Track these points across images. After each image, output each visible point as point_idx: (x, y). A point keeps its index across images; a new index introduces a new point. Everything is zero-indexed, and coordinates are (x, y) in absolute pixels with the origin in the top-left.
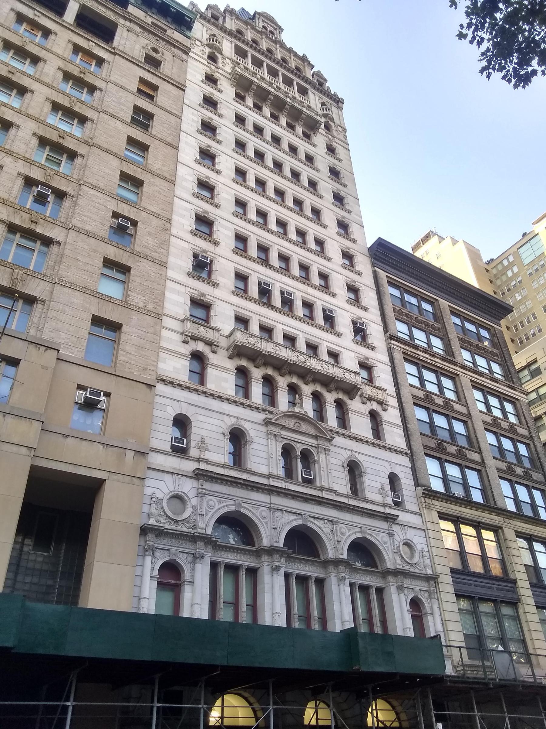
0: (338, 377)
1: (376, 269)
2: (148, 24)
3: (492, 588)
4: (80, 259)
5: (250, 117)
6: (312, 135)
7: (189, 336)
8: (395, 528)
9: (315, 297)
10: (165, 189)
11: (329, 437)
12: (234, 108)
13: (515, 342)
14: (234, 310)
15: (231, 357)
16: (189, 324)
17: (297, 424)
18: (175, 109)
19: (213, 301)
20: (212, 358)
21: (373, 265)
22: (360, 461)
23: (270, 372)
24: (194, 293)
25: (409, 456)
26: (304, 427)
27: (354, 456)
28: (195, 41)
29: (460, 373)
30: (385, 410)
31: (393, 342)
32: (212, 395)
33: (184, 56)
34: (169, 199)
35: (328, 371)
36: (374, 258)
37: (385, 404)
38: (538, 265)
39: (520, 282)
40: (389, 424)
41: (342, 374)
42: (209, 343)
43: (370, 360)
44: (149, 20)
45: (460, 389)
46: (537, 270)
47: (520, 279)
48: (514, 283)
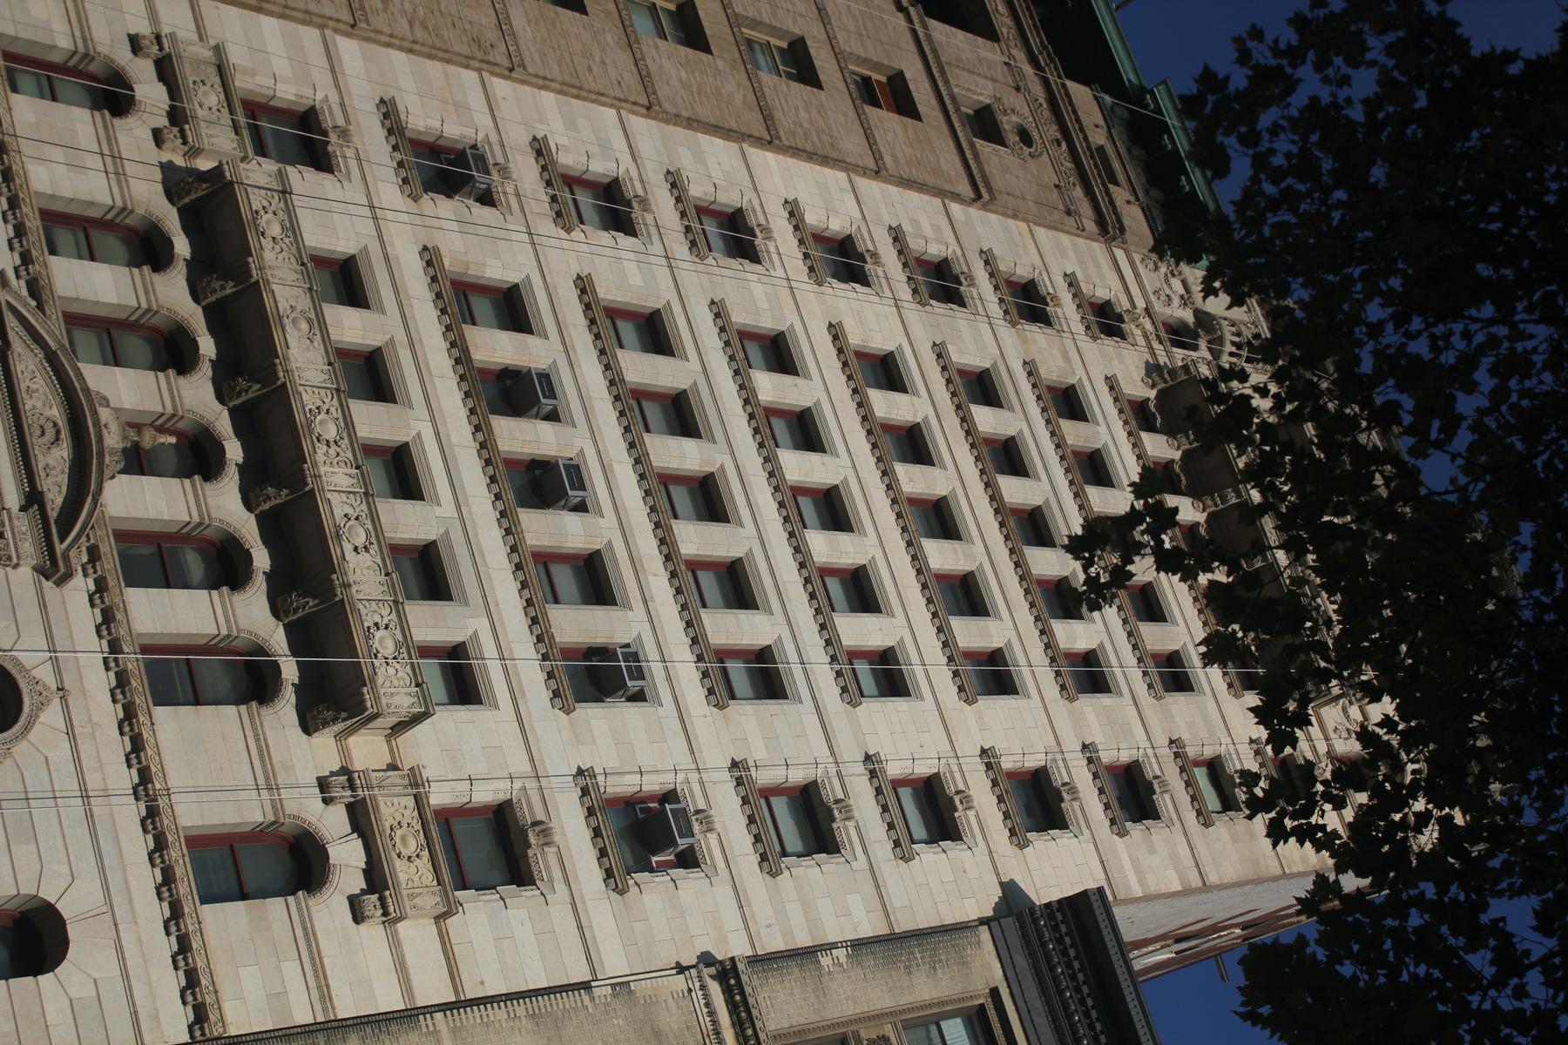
0: (347, 586)
2: (1089, 147)
5: (1102, 429)
7: (161, 49)
9: (645, 602)
10: (613, 74)
11: (60, 548)
12: (1080, 373)
14: (366, 248)
15: (175, 182)
16: (207, 54)
17: (50, 433)
18: (895, 158)
19: (349, 173)
20: (134, 133)
22: (27, 728)
23: (290, 670)
24: (331, 113)
25: (198, 1033)
26: (55, 461)
27: (41, 706)
28: (1173, 275)
30: (358, 914)
31: (715, 988)
32: (137, 745)
33: (1091, 226)
34: (591, 79)
35: (348, 547)
37: (382, 900)
40: (300, 933)
41: (377, 619)
42: (177, 117)
43: (551, 850)
44: (1099, 138)
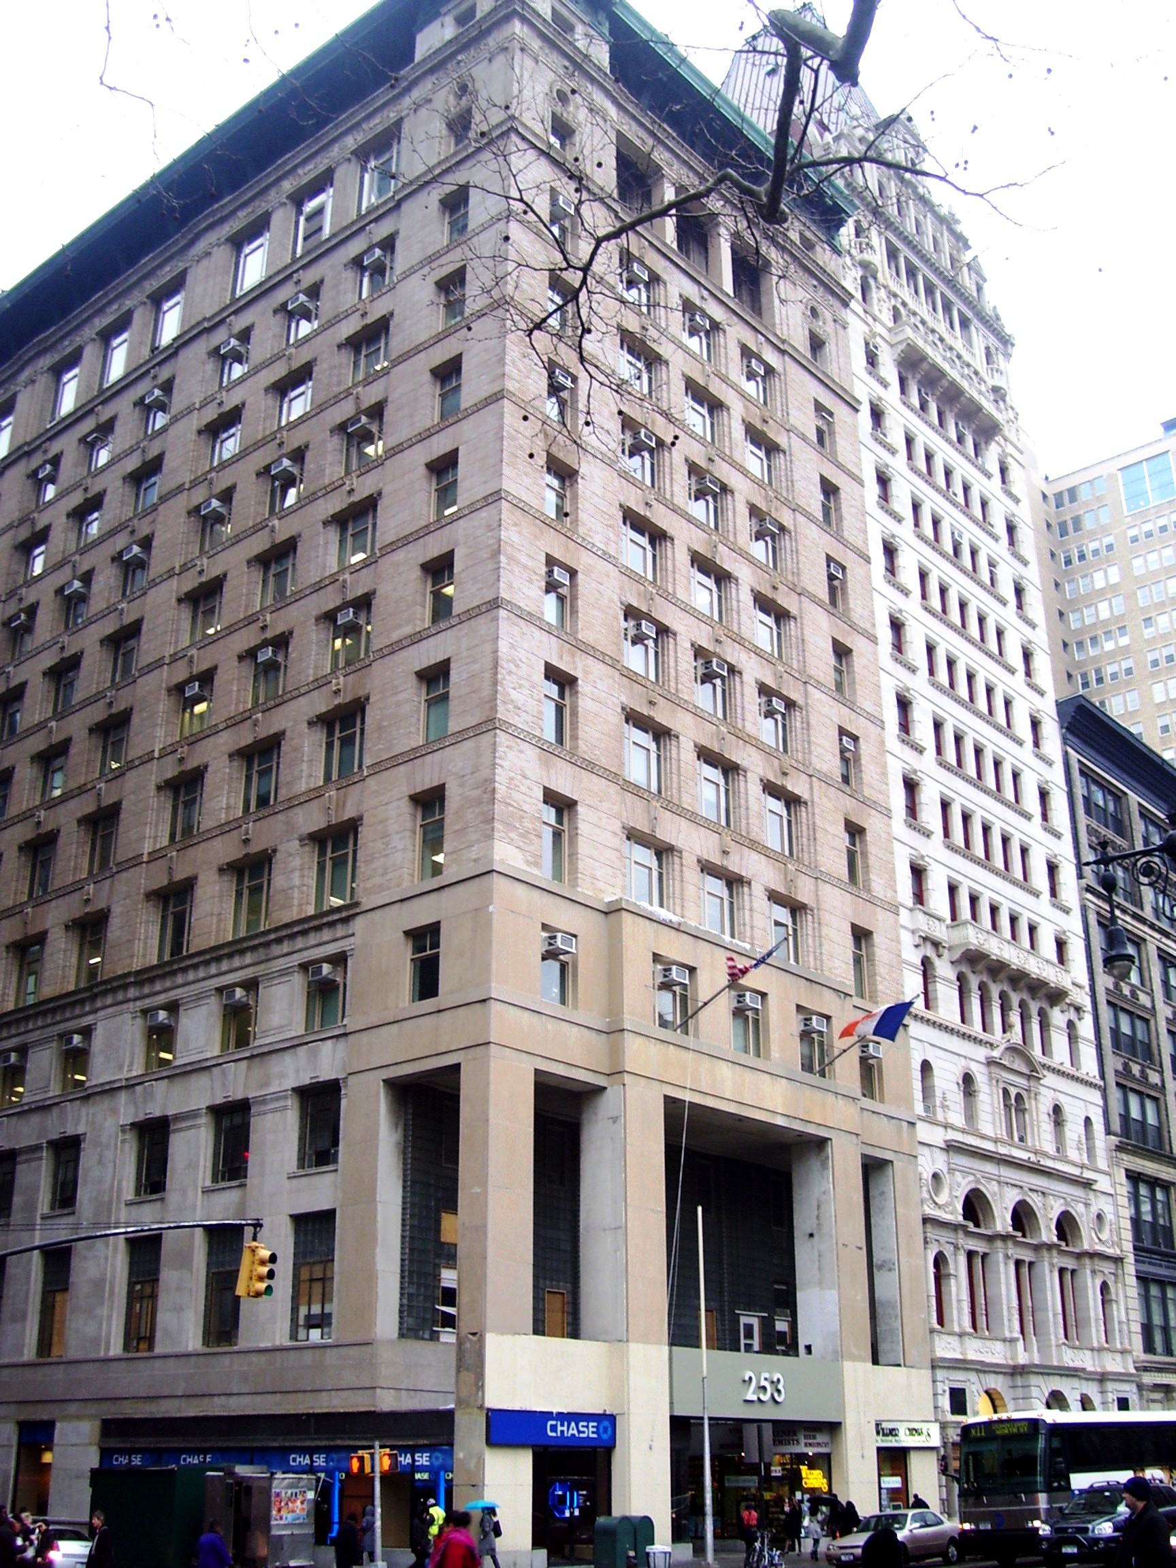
1: (1070, 750)
3: (1160, 1266)
4: (827, 827)
6: (983, 446)
8: (1091, 1195)
13: (1074, 679)
20: (937, 962)
21: (1065, 741)
29: (1148, 938)
36: (1067, 728)
38: (1155, 524)
39: (1110, 547)
45: (1145, 965)
46: (1149, 535)
47: (1107, 540)
48: (1093, 545)
